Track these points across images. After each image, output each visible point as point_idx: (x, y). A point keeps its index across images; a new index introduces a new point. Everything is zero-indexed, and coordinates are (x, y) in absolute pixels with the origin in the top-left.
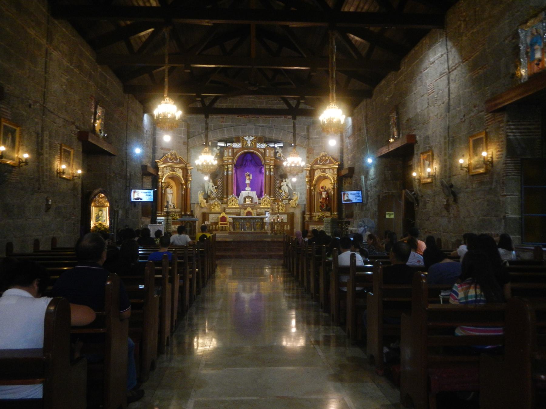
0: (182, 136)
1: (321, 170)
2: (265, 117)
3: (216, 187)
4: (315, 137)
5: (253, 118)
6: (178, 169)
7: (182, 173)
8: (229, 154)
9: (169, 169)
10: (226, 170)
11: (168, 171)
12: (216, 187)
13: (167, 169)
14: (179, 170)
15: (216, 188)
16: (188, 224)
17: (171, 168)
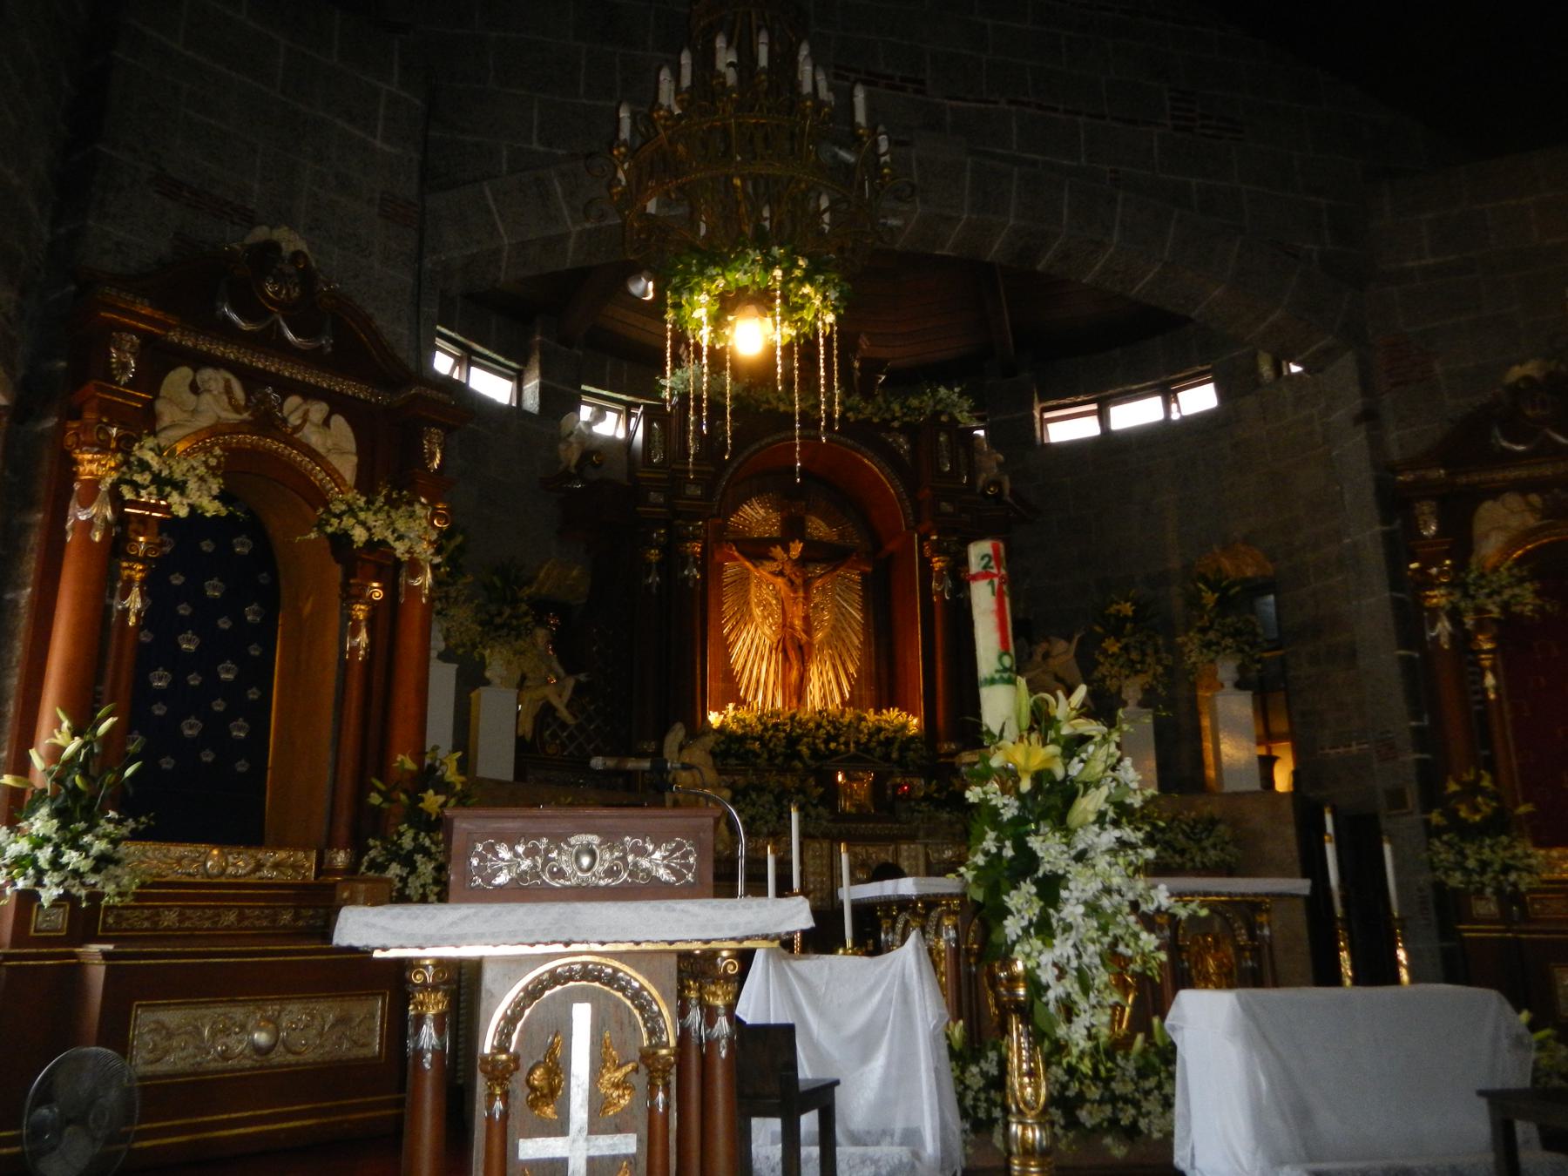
0: (378, 143)
1: (1535, 499)
2: (1039, 107)
3: (582, 677)
4: (1430, 261)
5: (954, 103)
6: (318, 410)
7: (355, 459)
9: (228, 390)
10: (654, 555)
12: (582, 677)
13: (195, 389)
14: (326, 423)
15: (579, 690)
16: (582, 1015)
17: (248, 392)
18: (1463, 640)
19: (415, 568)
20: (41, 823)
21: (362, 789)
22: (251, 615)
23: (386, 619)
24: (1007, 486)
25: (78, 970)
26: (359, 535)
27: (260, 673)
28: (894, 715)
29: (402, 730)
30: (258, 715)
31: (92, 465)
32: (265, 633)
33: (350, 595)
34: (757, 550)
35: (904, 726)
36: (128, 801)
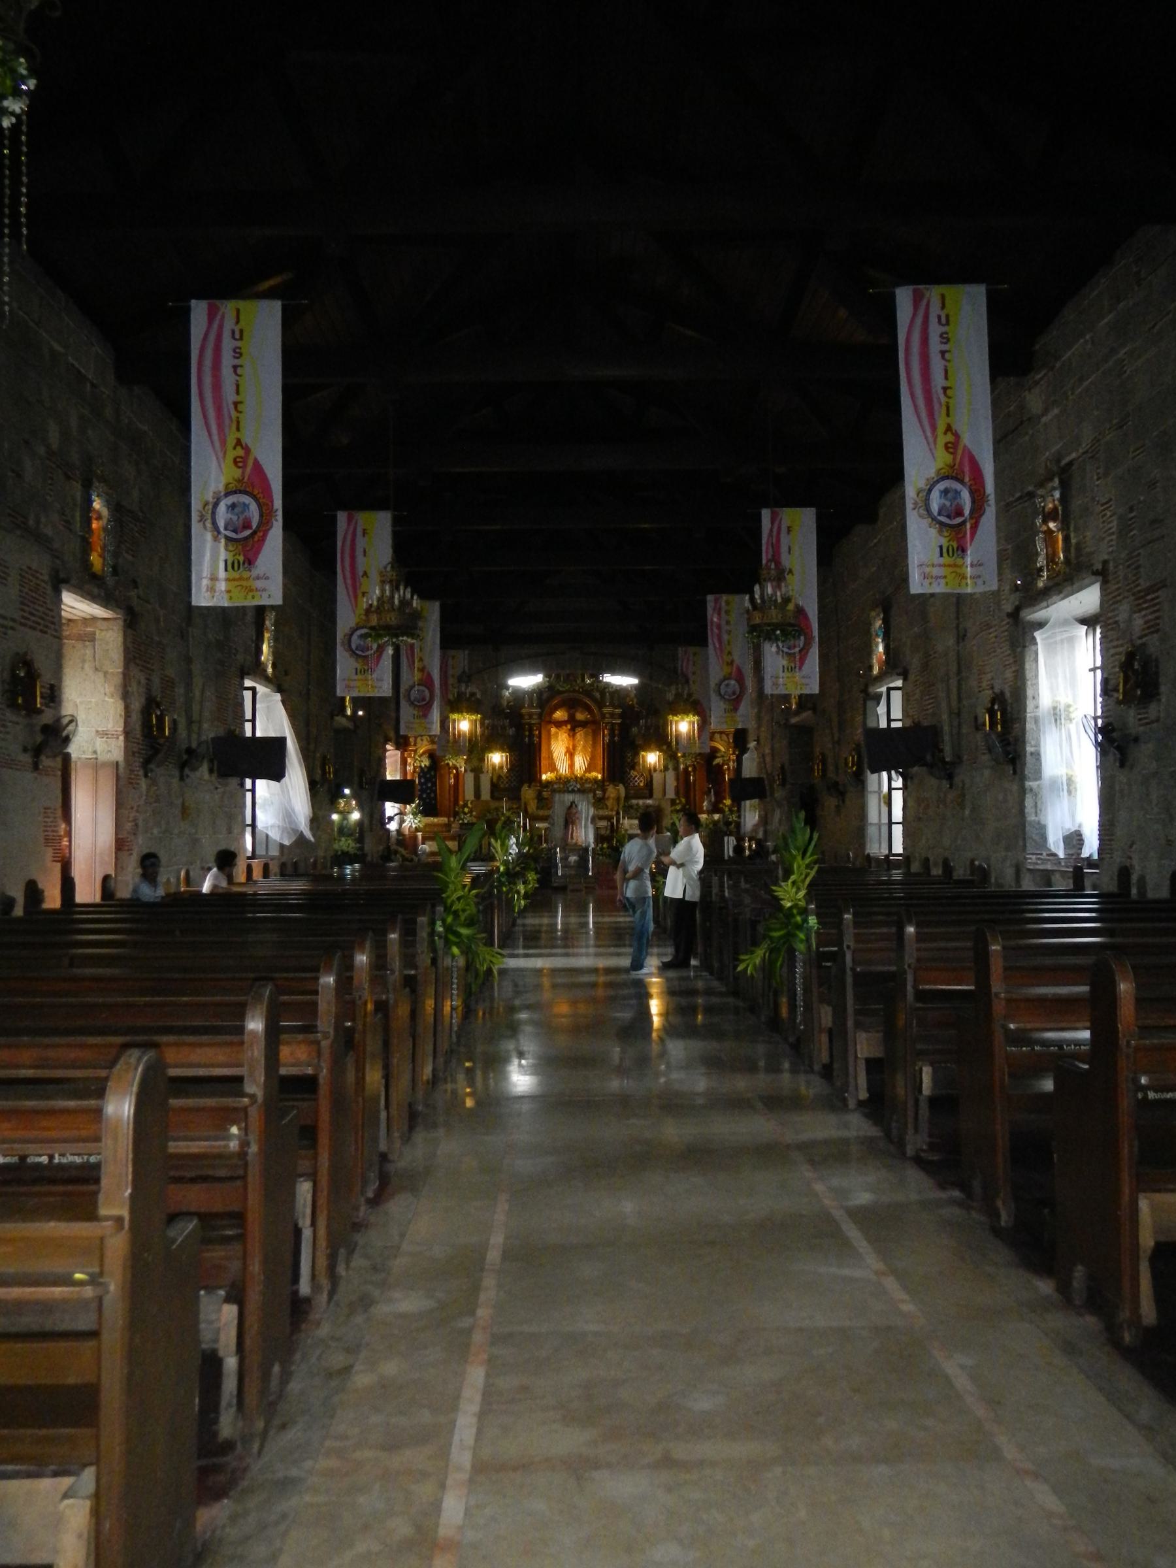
8: (533, 704)
11: (425, 742)
13: (422, 740)
18: (686, 769)
19: (461, 767)
20: (411, 816)
21: (455, 808)
22: (433, 773)
23: (457, 776)
24: (635, 700)
25: (416, 837)
26: (451, 764)
27: (434, 784)
28: (594, 774)
29: (460, 797)
30: (435, 792)
31: (409, 760)
32: (435, 776)
33: (450, 773)
34: (559, 724)
35: (597, 777)
36: (420, 812)
